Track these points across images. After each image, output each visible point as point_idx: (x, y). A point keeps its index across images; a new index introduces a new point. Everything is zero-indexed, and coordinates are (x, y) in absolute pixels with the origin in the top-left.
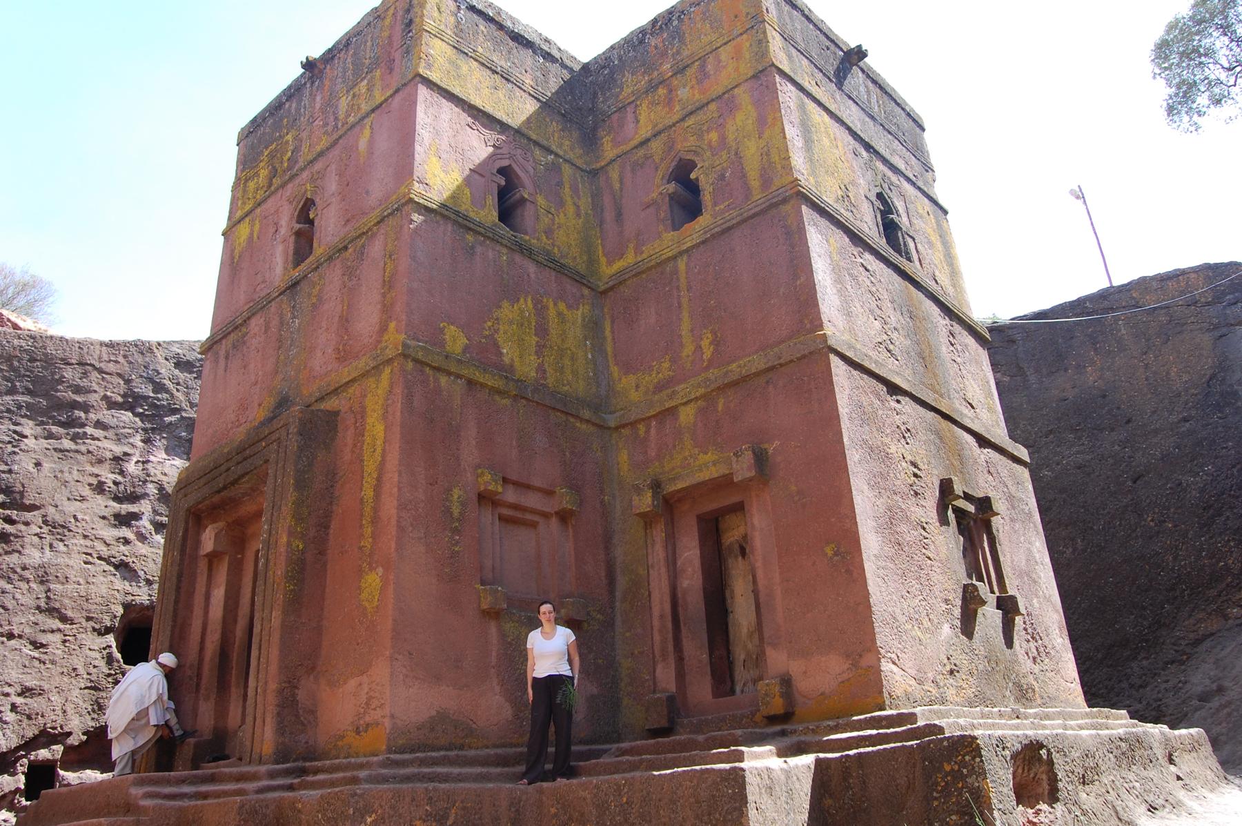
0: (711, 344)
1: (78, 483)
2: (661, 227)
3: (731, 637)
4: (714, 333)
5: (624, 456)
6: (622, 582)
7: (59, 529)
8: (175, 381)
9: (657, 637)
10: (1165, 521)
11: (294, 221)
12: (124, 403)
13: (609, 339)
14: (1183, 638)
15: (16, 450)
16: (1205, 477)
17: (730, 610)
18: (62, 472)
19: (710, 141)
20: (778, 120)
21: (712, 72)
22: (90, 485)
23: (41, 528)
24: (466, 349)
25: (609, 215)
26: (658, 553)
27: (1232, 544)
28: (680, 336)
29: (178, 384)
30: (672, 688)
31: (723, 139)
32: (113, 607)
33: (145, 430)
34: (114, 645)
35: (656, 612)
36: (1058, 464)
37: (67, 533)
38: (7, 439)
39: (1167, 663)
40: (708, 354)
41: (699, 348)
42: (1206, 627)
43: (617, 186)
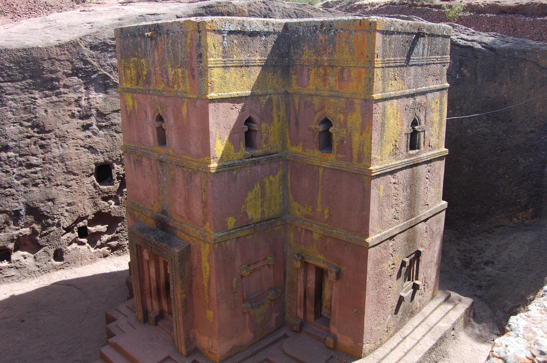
0: (328, 214)
1: (64, 116)
2: (314, 146)
3: (322, 297)
4: (330, 211)
5: (292, 235)
6: (288, 279)
7: (62, 138)
8: (92, 57)
9: (298, 301)
10: (506, 174)
11: (155, 121)
12: (73, 73)
13: (289, 181)
14: (493, 223)
15: (35, 106)
16: (528, 163)
17: (323, 289)
18: (56, 112)
19: (340, 119)
20: (370, 131)
21: (346, 79)
22: (69, 115)
23: (55, 139)
24: (235, 223)
25: (293, 121)
26: (301, 277)
27: (525, 195)
28: (317, 202)
29: (94, 58)
30: (302, 317)
31: (345, 122)
32: (91, 166)
33: (84, 83)
34: (95, 179)
35: (299, 294)
36: (475, 129)
37: (66, 139)
38: (30, 102)
39: (484, 231)
40: (326, 217)
41: (323, 212)
42: (503, 222)
43: (297, 108)
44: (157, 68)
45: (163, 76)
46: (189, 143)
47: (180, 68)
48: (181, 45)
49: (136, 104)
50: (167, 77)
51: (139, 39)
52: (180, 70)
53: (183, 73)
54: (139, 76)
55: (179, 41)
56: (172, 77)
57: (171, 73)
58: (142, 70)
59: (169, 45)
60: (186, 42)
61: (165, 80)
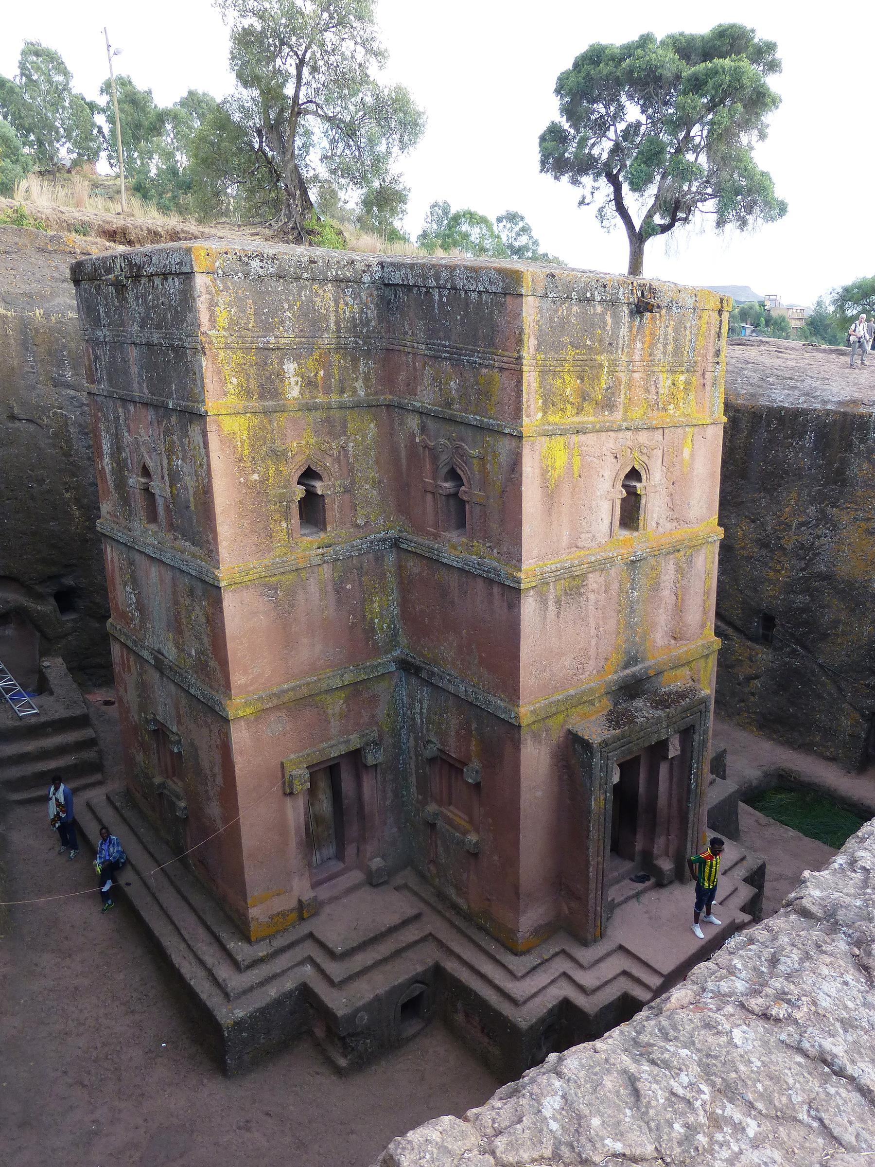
44: (635, 375)
45: (647, 391)
46: (688, 504)
47: (682, 372)
48: (691, 332)
49: (577, 460)
50: (657, 393)
51: (599, 309)
52: (682, 378)
53: (687, 383)
54: (584, 397)
55: (688, 325)
56: (666, 391)
57: (664, 381)
58: (596, 378)
59: (670, 330)
60: (699, 329)
61: (650, 397)
